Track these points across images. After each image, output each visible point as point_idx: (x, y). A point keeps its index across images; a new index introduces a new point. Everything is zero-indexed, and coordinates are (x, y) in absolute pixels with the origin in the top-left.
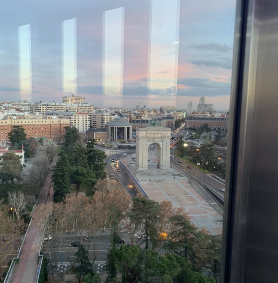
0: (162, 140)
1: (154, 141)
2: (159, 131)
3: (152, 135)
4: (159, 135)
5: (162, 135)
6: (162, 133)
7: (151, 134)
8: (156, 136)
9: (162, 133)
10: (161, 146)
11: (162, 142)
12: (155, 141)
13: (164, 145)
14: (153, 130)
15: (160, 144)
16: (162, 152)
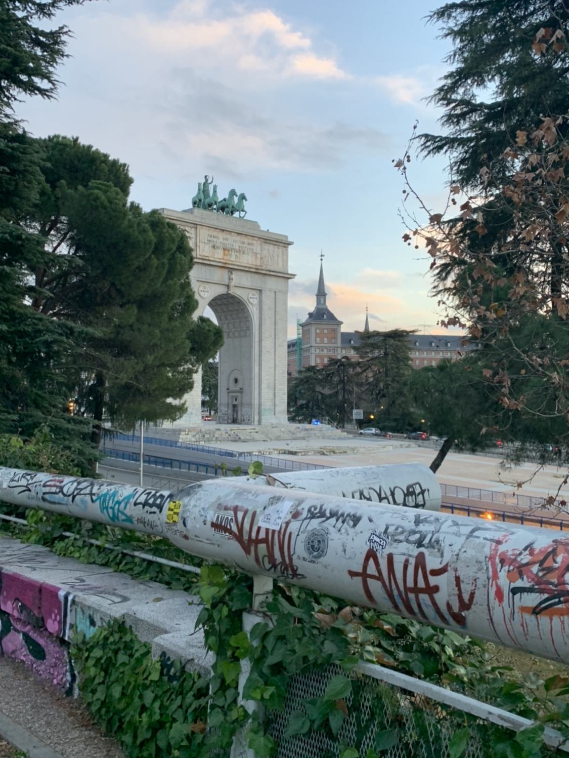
0: (256, 282)
1: (228, 286)
2: (246, 240)
3: (219, 255)
4: (247, 260)
5: (258, 263)
6: (259, 251)
8: (233, 258)
9: (259, 251)
10: (254, 311)
11: (257, 295)
12: (233, 283)
13: (265, 308)
14: (223, 230)
15: (251, 301)
16: (260, 341)
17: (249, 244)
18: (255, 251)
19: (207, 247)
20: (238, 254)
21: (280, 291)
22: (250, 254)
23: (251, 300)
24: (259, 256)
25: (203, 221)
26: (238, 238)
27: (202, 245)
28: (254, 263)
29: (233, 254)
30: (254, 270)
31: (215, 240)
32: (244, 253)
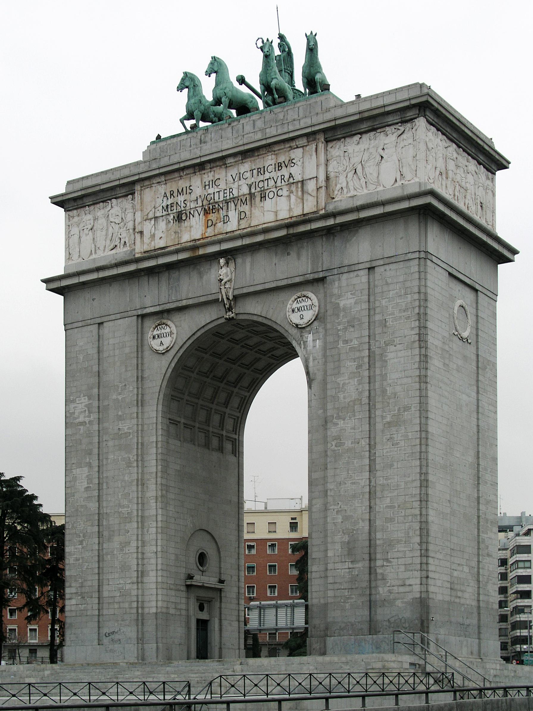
5: (310, 206)
7: (179, 218)
9: (310, 172)
17: (279, 166)
18: (298, 177)
19: (162, 224)
20: (246, 208)
21: (390, 260)
22: (285, 192)
23: (295, 318)
24: (311, 186)
25: (154, 166)
26: (245, 167)
27: (148, 227)
28: (297, 211)
29: (233, 215)
30: (282, 233)
31: (181, 199)
32: (263, 197)
